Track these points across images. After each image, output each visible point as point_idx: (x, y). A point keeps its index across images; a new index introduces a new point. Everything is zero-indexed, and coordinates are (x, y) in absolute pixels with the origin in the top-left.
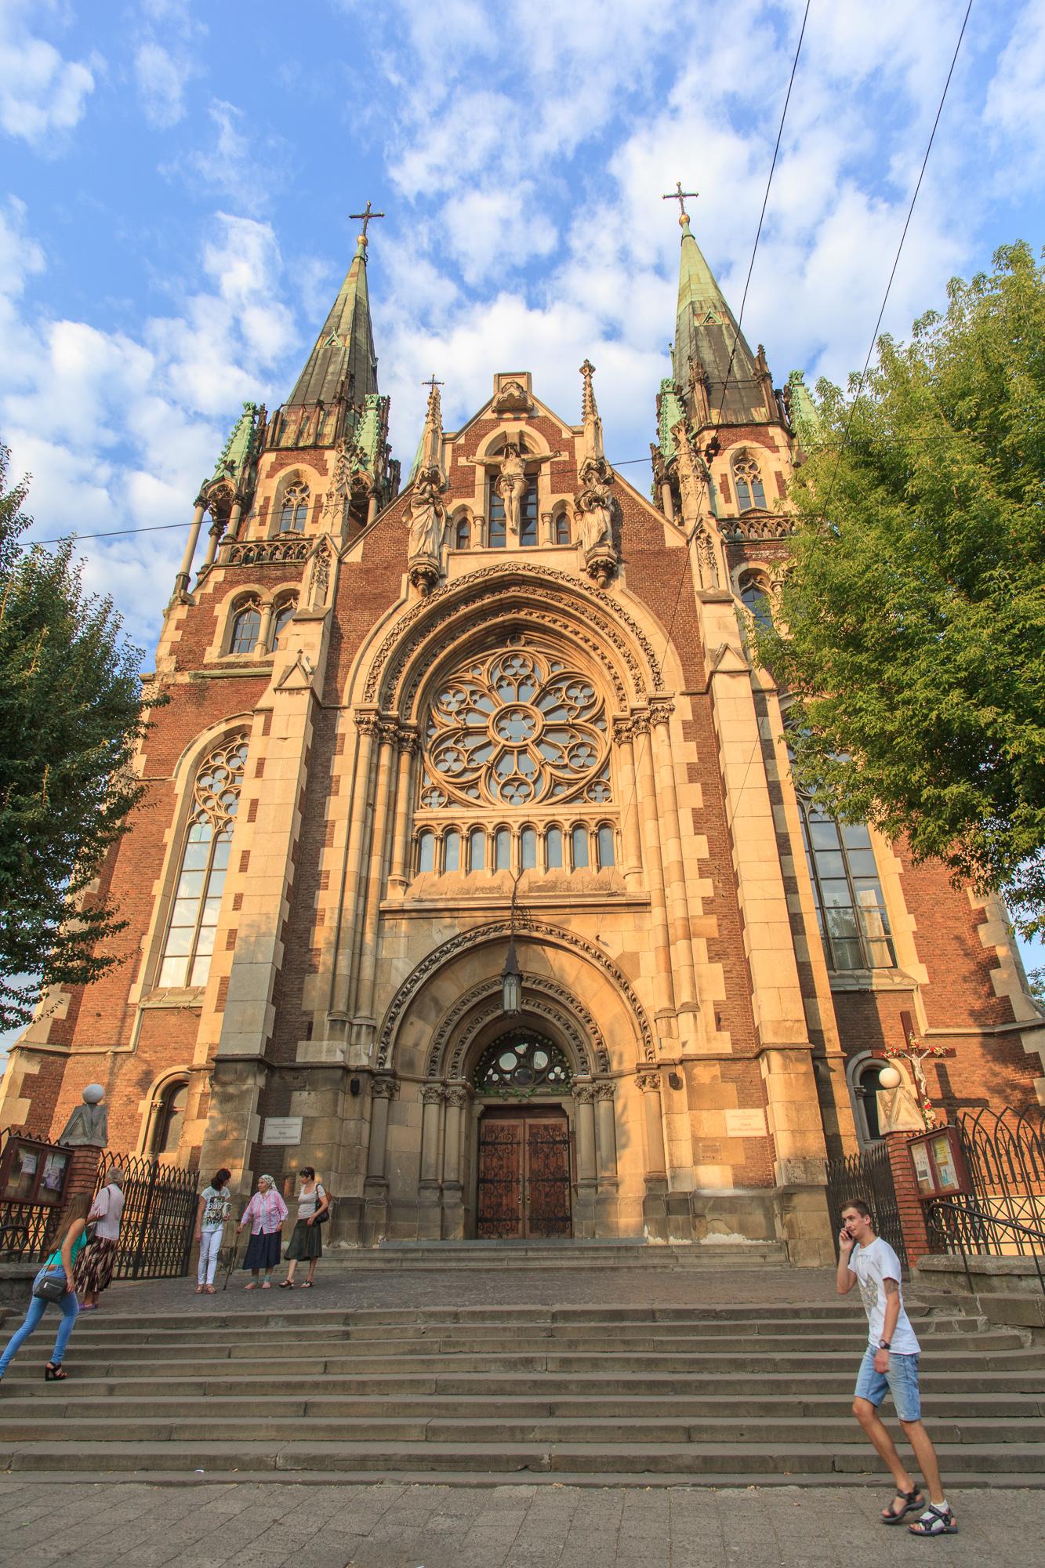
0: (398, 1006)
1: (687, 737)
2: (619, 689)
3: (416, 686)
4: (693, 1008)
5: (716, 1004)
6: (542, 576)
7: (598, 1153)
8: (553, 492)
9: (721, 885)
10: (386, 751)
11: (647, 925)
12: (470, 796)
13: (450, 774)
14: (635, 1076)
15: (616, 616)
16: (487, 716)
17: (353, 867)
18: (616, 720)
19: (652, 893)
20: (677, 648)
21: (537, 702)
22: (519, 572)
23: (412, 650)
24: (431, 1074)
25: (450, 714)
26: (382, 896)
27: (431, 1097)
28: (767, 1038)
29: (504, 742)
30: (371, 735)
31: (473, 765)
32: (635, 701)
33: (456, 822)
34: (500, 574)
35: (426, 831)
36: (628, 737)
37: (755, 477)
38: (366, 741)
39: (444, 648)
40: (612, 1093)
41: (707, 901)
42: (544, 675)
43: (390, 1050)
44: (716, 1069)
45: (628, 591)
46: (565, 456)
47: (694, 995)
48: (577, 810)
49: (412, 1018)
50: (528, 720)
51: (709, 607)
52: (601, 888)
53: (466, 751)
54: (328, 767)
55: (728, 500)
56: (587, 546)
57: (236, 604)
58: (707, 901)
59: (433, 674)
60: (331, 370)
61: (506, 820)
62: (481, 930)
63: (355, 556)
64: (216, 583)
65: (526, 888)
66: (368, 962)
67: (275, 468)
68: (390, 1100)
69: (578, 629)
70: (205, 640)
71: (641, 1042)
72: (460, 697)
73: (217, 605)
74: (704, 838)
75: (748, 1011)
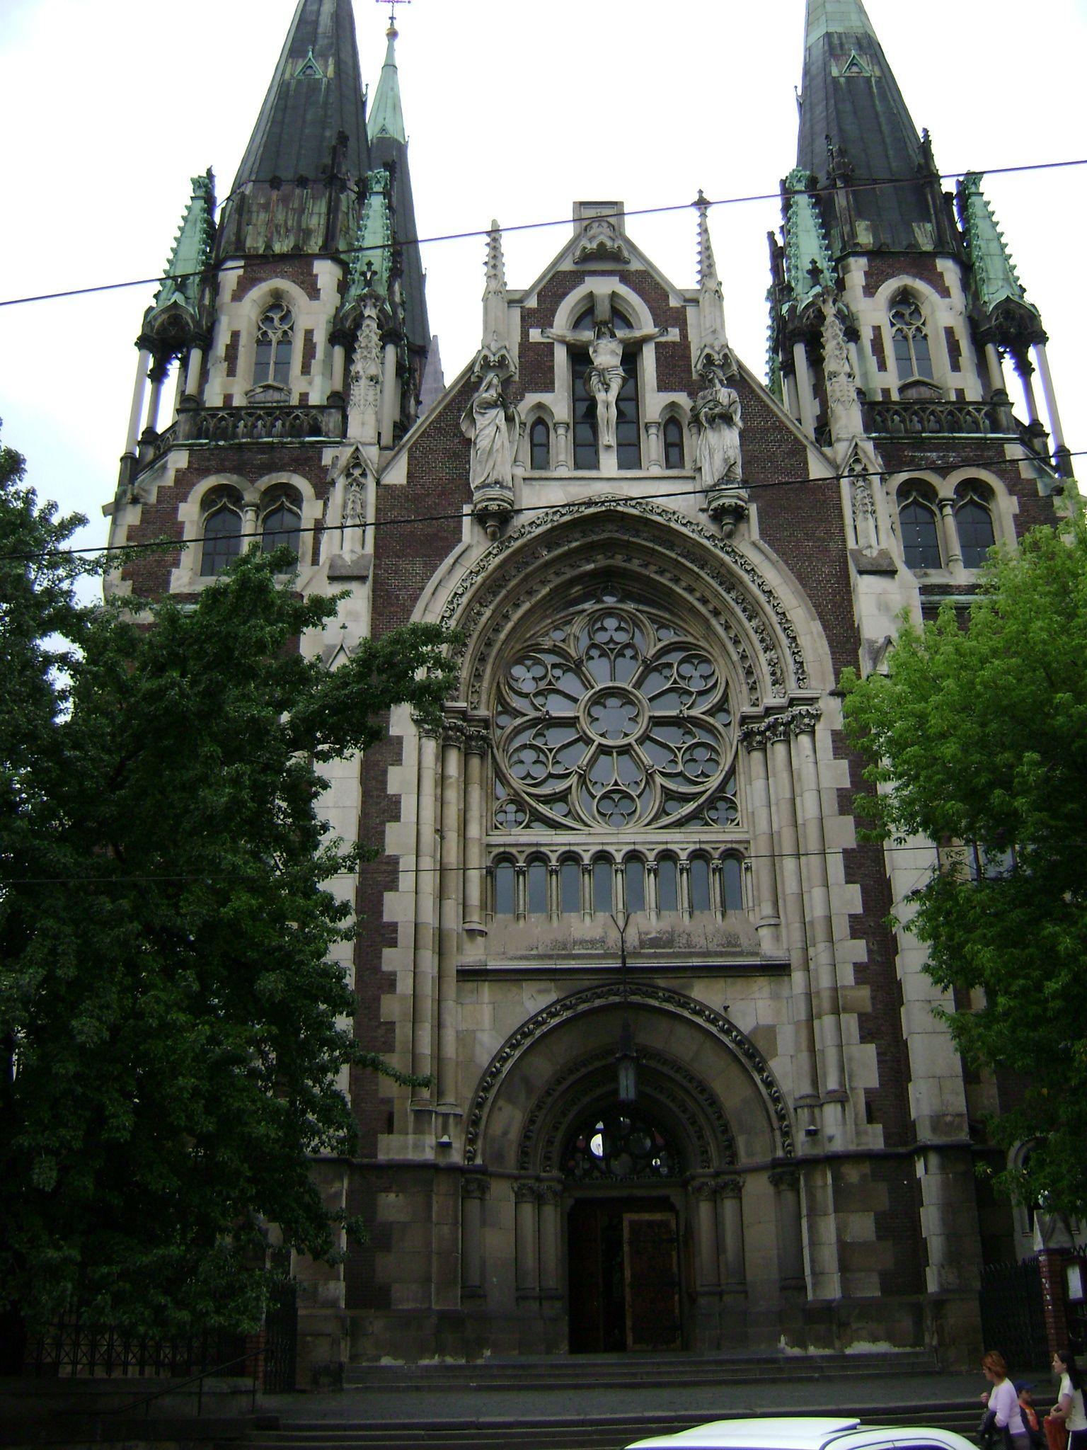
0: (486, 1090)
1: (838, 752)
2: (749, 672)
3: (482, 659)
4: (841, 1098)
6: (649, 516)
8: (660, 389)
9: (875, 948)
10: (453, 758)
14: (769, 1173)
15: (746, 578)
16: (575, 700)
17: (429, 916)
18: (744, 720)
20: (825, 627)
21: (638, 685)
23: (479, 614)
24: (525, 1169)
25: (526, 695)
27: (524, 1195)
28: (925, 1135)
29: (599, 740)
31: (559, 770)
33: (543, 849)
35: (505, 858)
36: (760, 742)
37: (918, 329)
38: (430, 746)
39: (517, 606)
40: (740, 1191)
42: (650, 643)
43: (480, 1143)
44: (866, 1168)
46: (674, 335)
47: (842, 1084)
49: (501, 1103)
50: (628, 707)
51: (865, 577)
52: (729, 944)
53: (551, 750)
54: (384, 783)
55: (882, 366)
56: (708, 478)
57: (207, 502)
58: (858, 968)
60: (309, 117)
61: (607, 848)
62: (583, 995)
63: (397, 475)
64: (178, 471)
65: (637, 943)
66: (449, 1036)
69: (694, 585)
71: (778, 1133)
72: (539, 671)
73: (182, 506)
74: (857, 887)
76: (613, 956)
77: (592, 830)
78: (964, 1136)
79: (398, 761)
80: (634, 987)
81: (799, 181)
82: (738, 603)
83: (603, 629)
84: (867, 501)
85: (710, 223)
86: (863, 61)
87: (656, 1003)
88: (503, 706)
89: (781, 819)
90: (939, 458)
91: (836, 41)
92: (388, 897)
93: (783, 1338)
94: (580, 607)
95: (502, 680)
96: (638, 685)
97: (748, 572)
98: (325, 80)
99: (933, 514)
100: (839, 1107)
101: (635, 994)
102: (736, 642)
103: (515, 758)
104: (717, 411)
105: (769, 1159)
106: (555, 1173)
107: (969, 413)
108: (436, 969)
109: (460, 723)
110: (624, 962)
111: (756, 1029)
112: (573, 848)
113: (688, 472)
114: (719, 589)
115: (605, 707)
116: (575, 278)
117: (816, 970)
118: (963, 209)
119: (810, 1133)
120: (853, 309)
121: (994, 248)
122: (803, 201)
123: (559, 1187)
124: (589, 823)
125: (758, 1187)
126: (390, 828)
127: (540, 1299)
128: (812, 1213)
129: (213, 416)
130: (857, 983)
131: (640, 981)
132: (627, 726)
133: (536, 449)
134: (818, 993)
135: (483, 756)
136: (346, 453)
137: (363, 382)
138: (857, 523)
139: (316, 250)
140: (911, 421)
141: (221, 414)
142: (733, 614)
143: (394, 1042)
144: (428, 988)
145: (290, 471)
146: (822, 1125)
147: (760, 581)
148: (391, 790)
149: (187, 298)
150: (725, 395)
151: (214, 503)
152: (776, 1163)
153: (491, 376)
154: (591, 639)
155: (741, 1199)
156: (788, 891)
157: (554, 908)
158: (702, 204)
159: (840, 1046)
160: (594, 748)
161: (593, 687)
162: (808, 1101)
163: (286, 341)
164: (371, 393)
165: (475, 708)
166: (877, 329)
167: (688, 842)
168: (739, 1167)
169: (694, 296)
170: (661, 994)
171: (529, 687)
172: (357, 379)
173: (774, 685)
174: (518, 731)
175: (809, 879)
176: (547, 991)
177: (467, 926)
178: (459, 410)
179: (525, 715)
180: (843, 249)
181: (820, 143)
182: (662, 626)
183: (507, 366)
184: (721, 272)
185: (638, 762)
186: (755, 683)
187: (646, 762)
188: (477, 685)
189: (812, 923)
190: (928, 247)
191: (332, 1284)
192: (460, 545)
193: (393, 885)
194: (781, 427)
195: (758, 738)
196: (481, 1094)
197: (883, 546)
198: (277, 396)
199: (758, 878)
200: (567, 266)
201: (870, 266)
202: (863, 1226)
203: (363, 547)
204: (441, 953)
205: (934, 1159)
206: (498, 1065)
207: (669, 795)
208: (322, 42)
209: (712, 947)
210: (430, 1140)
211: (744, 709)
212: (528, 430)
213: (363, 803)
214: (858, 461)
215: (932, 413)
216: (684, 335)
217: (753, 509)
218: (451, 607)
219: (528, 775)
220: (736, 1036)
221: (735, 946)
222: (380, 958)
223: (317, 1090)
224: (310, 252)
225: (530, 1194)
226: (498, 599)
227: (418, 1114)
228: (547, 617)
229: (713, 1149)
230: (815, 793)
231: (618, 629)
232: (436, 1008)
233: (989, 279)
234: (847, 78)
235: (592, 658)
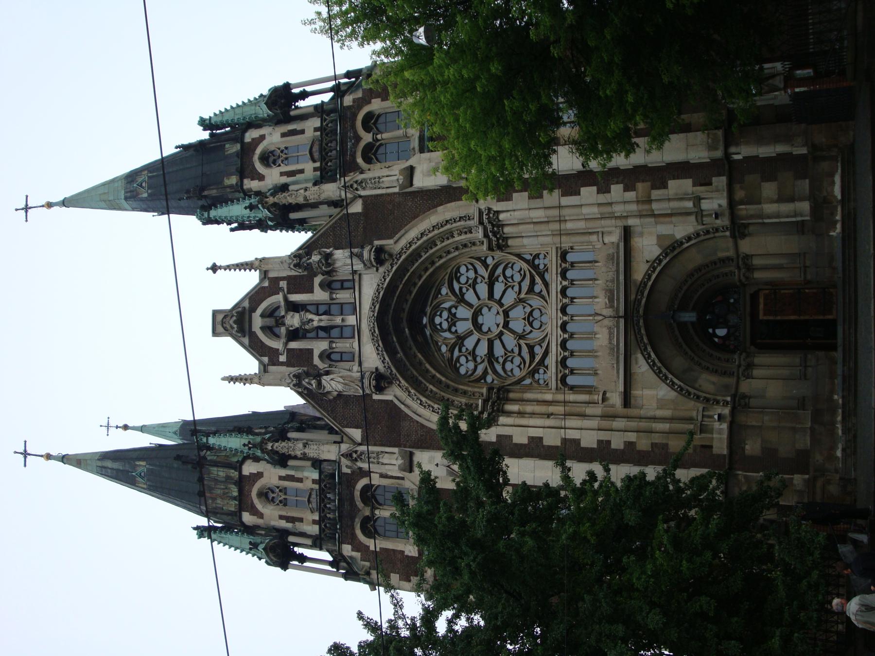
0: (690, 394)
1: (509, 198)
2: (465, 246)
3: (456, 390)
4: (698, 200)
5: (694, 186)
7: (785, 266)
8: (312, 292)
10: (509, 407)
11: (639, 229)
12: (539, 351)
13: (522, 366)
15: (414, 247)
16: (479, 340)
18: (490, 248)
19: (618, 225)
20: (441, 205)
22: (376, 315)
23: (431, 391)
24: (734, 373)
26: (613, 406)
28: (719, 154)
29: (500, 328)
30: (499, 416)
31: (516, 350)
32: (479, 234)
33: (559, 359)
34: (376, 330)
35: (563, 380)
36: (503, 241)
37: (282, 152)
38: (502, 420)
39: (427, 371)
40: (747, 255)
41: (626, 189)
43: (719, 398)
44: (737, 187)
45: (395, 238)
46: (283, 284)
47: (689, 199)
48: (553, 277)
49: (697, 386)
52: (613, 259)
53: (506, 354)
54: (521, 445)
55: (301, 171)
58: (626, 189)
59: (447, 378)
61: (559, 324)
62: (639, 339)
63: (356, 434)
64: (352, 550)
65: (611, 310)
66: (660, 413)
67: (255, 512)
68: (750, 397)
70: (399, 556)
71: (717, 235)
75: (700, 166)
76: (618, 323)
77: (550, 332)
78: (720, 133)
79: (510, 437)
80: (635, 312)
81: (203, 215)
82: (427, 252)
83: (440, 324)
84: (373, 181)
85: (223, 264)
86: (140, 180)
87: (644, 300)
88: (481, 380)
89: (545, 229)
90: (351, 141)
91: (129, 194)
92: (584, 444)
93: (831, 234)
94: (429, 336)
95: (467, 380)
96: (470, 305)
97: (410, 246)
98: (147, 466)
99: (381, 145)
100: (702, 201)
101: (639, 311)
102: (449, 252)
103: (510, 373)
104: (324, 262)
105: (731, 239)
106: (736, 356)
107: (327, 125)
108: (623, 419)
109: (490, 403)
110: (621, 317)
111: (660, 246)
112: (559, 343)
113: (356, 277)
114: (420, 261)
115: (483, 324)
116: (253, 336)
117: (627, 212)
118: (218, 127)
119: (717, 217)
120: (271, 187)
121: (238, 111)
122: (213, 213)
123: (744, 355)
124: (545, 334)
125: (746, 246)
126: (546, 442)
127: (806, 367)
128: (761, 216)
129: (324, 531)
130: (635, 190)
131: (632, 308)
132: (494, 311)
133: (343, 359)
134: (640, 211)
135: (509, 391)
136: (344, 462)
137: (307, 451)
138: (385, 186)
139: (236, 473)
140: (331, 156)
141: (323, 526)
142: (433, 254)
143: (663, 444)
144: (633, 424)
145: (354, 491)
146: (711, 210)
147: (416, 239)
148: (525, 441)
149: (261, 543)
150: (315, 258)
151: (370, 531)
152: (733, 236)
153: (305, 383)
154: (446, 331)
155: (752, 255)
156: (584, 227)
157: (591, 354)
158: (214, 268)
159: (669, 200)
160: (505, 331)
161: (472, 331)
162: (699, 218)
163: (284, 490)
164: (312, 447)
165: (482, 395)
166: (282, 174)
167: (557, 281)
168: (735, 256)
169: (263, 272)
170: (639, 297)
171: (471, 365)
172: (305, 454)
173: (472, 233)
174: (495, 372)
175: (578, 215)
176: (636, 359)
177: (600, 402)
178: (322, 400)
179: (486, 368)
180: (239, 192)
181: (183, 203)
182: (439, 292)
183: (299, 374)
184: (250, 258)
185: (513, 307)
186: (470, 243)
187: (513, 302)
188: (470, 393)
189: (601, 214)
190: (237, 147)
191: (795, 482)
192: (394, 401)
193: (577, 442)
194: (333, 228)
195: (500, 241)
196: (692, 396)
197: (397, 172)
198: (314, 496)
199: (577, 243)
200: (246, 341)
201: (248, 178)
202: (769, 189)
203: (395, 453)
204: (614, 417)
205: (733, 149)
206: (676, 387)
207: (531, 290)
208: (127, 468)
209: (614, 269)
210: (717, 425)
211: (485, 249)
212: (333, 363)
213: (532, 456)
214: (352, 186)
215: (327, 144)
216: (283, 279)
217: (377, 243)
218: (427, 407)
219: (519, 366)
220: (663, 256)
221: (614, 256)
222: (617, 450)
223: (689, 492)
224: (237, 477)
225: (748, 369)
226: (423, 381)
227: (701, 432)
228: (434, 355)
229: (726, 270)
230: (531, 211)
231: (441, 316)
232: (644, 420)
233: (255, 114)
234: (149, 188)
235: (456, 330)
